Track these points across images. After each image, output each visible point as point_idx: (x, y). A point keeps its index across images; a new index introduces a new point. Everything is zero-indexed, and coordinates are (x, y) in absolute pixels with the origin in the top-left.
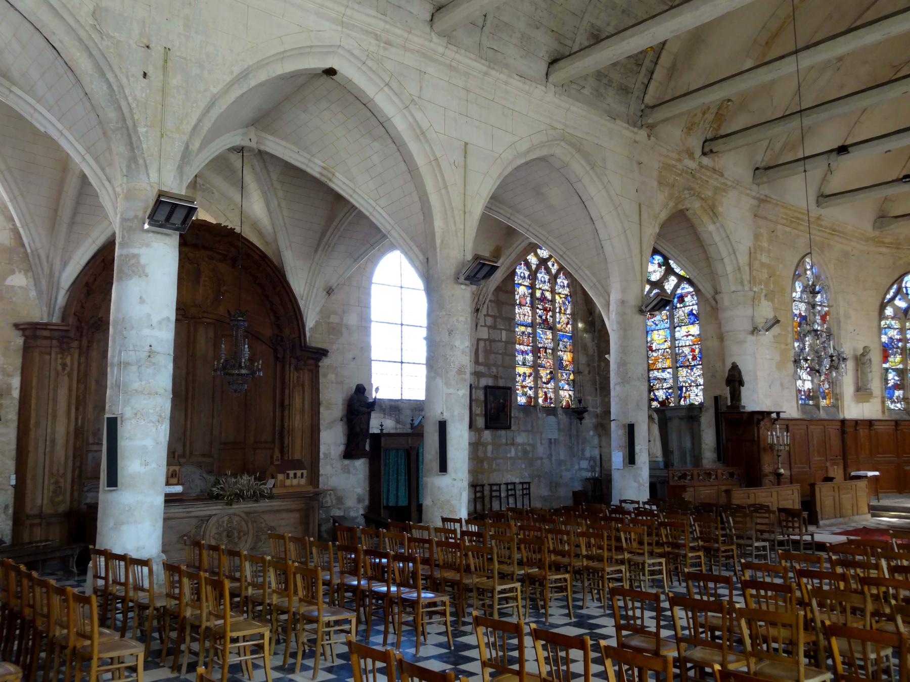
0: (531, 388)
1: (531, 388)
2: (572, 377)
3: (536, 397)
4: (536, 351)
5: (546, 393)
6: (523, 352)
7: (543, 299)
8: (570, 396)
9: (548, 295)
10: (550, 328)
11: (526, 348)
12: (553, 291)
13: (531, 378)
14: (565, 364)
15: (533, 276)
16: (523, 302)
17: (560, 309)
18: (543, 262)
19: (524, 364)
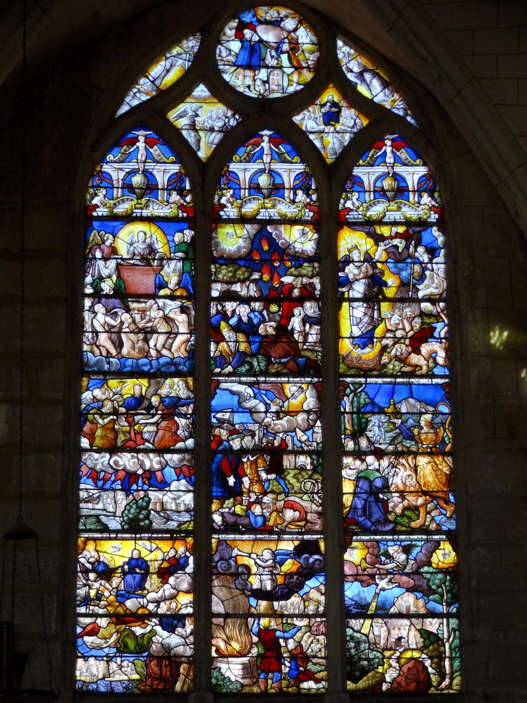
0: (171, 621)
1: (171, 621)
2: (445, 555)
3: (203, 659)
4: (212, 469)
5: (268, 638)
6: (129, 480)
7: (266, 253)
8: (430, 640)
9: (301, 240)
10: (302, 367)
11: (152, 461)
12: (328, 221)
13: (183, 580)
14: (396, 503)
15: (204, 178)
16: (144, 281)
17: (376, 282)
18: (262, 118)
19: (136, 526)
